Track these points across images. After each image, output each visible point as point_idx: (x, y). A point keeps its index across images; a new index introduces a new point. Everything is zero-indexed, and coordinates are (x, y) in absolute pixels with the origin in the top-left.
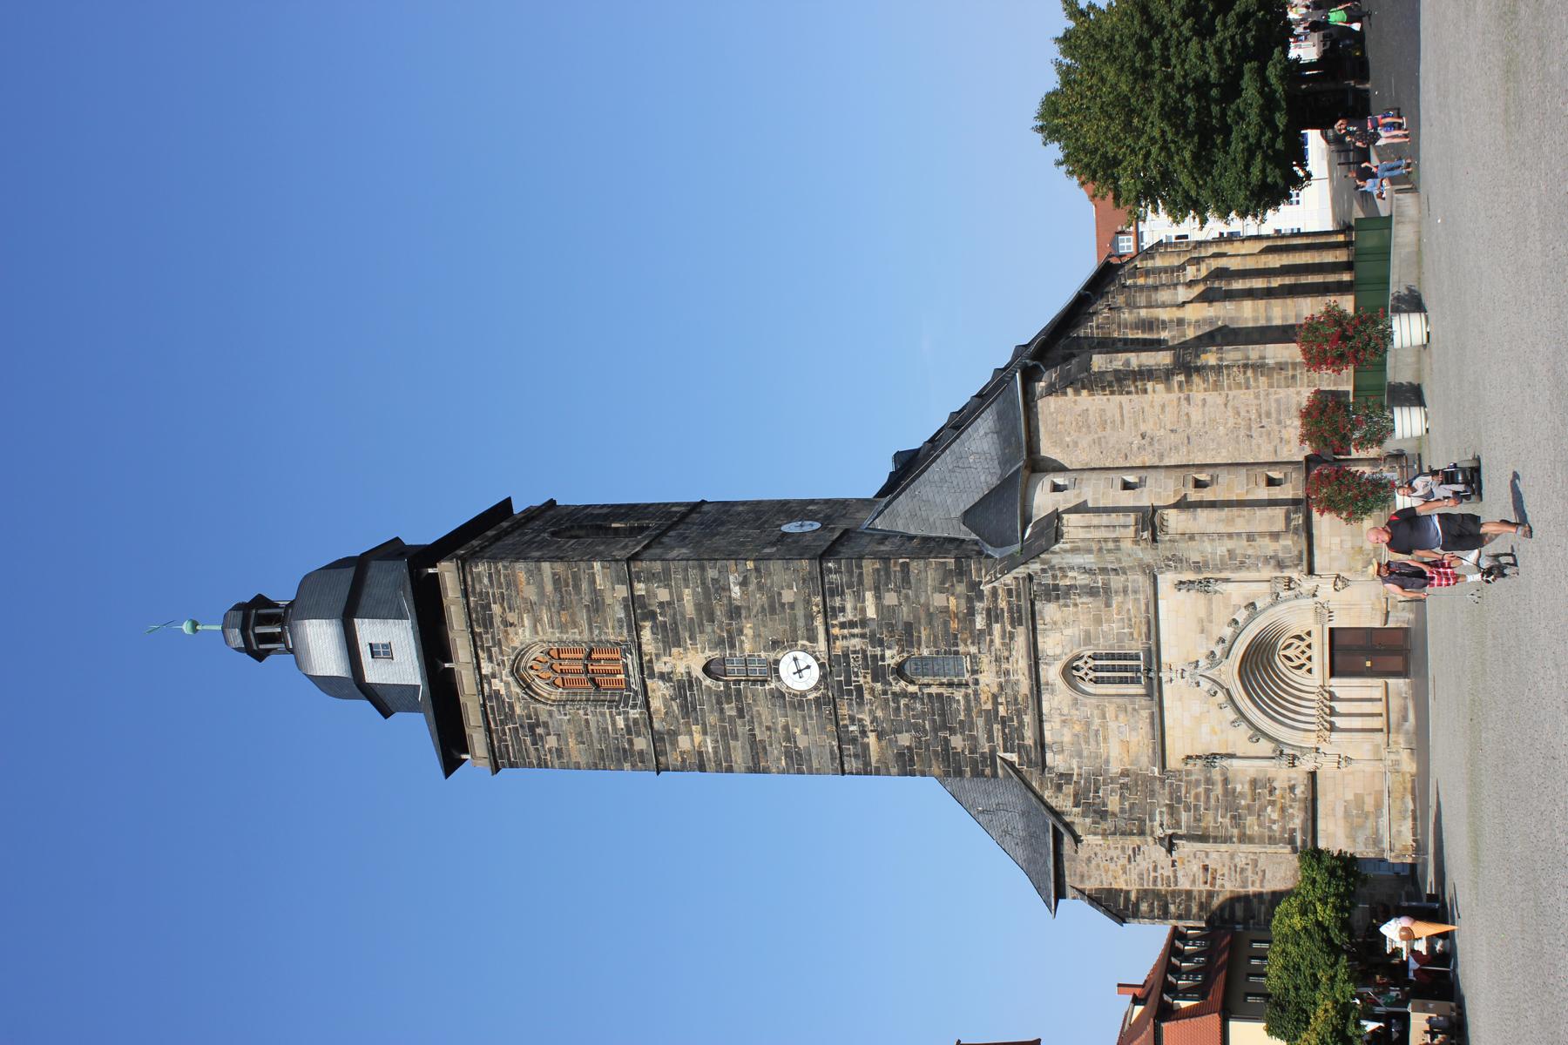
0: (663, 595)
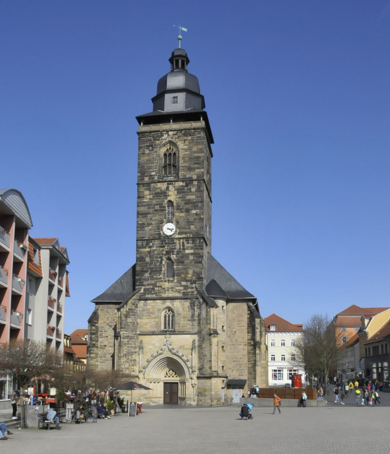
0: (193, 190)
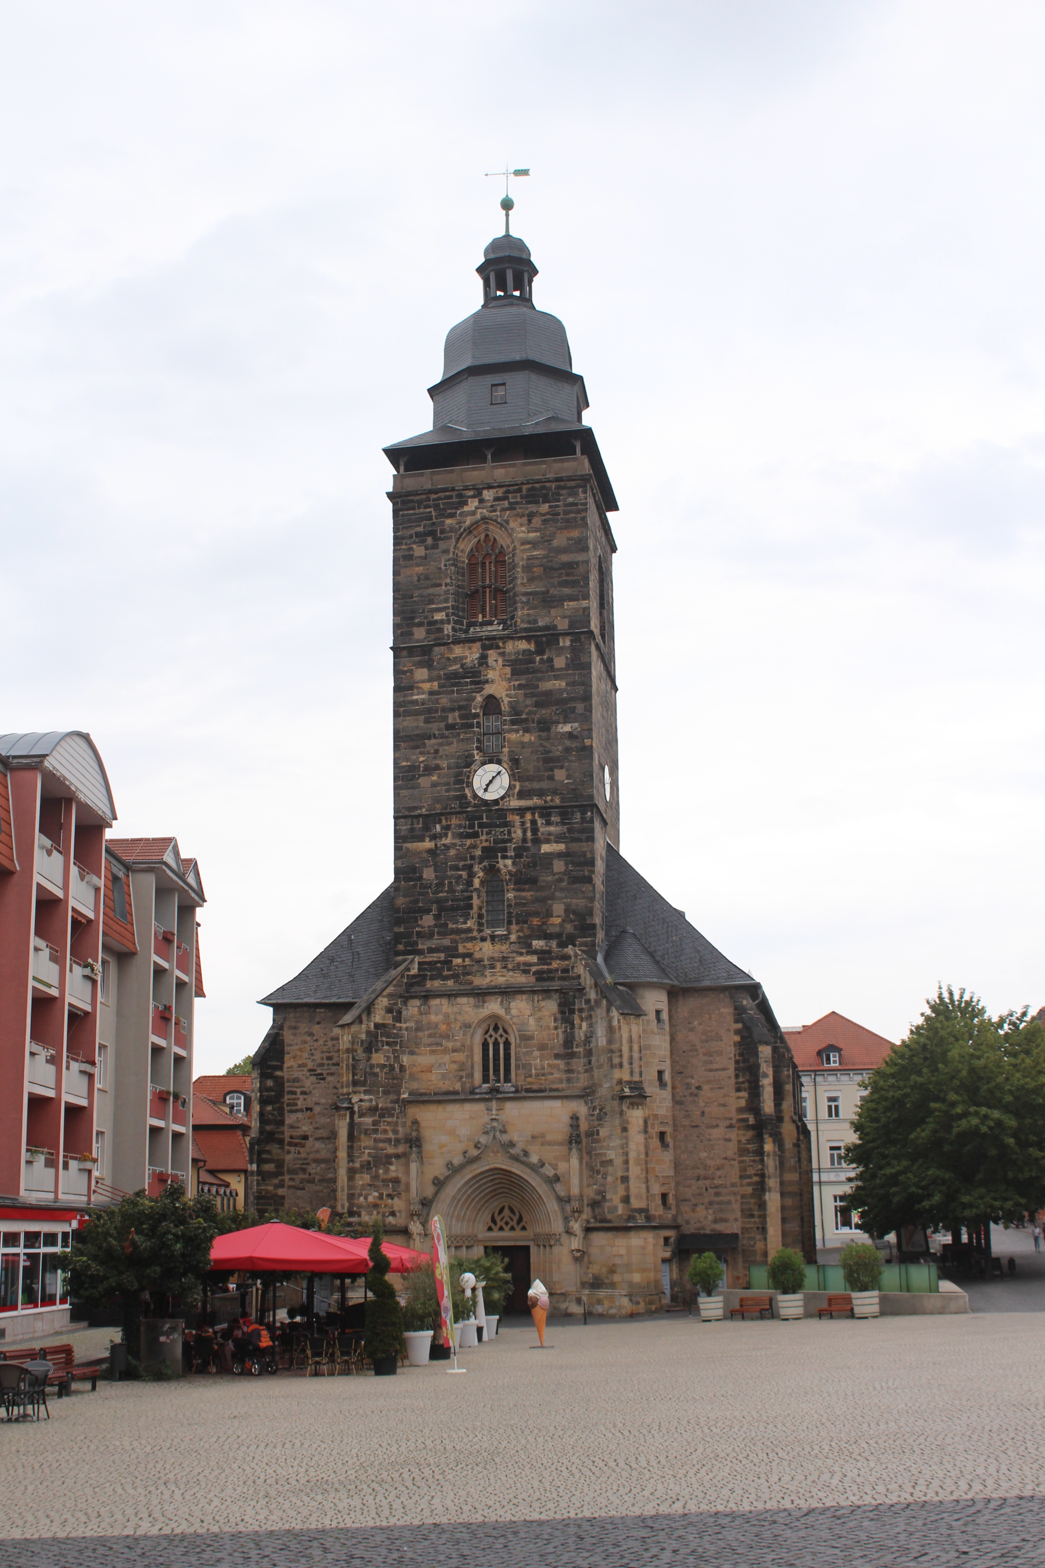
0: (560, 662)
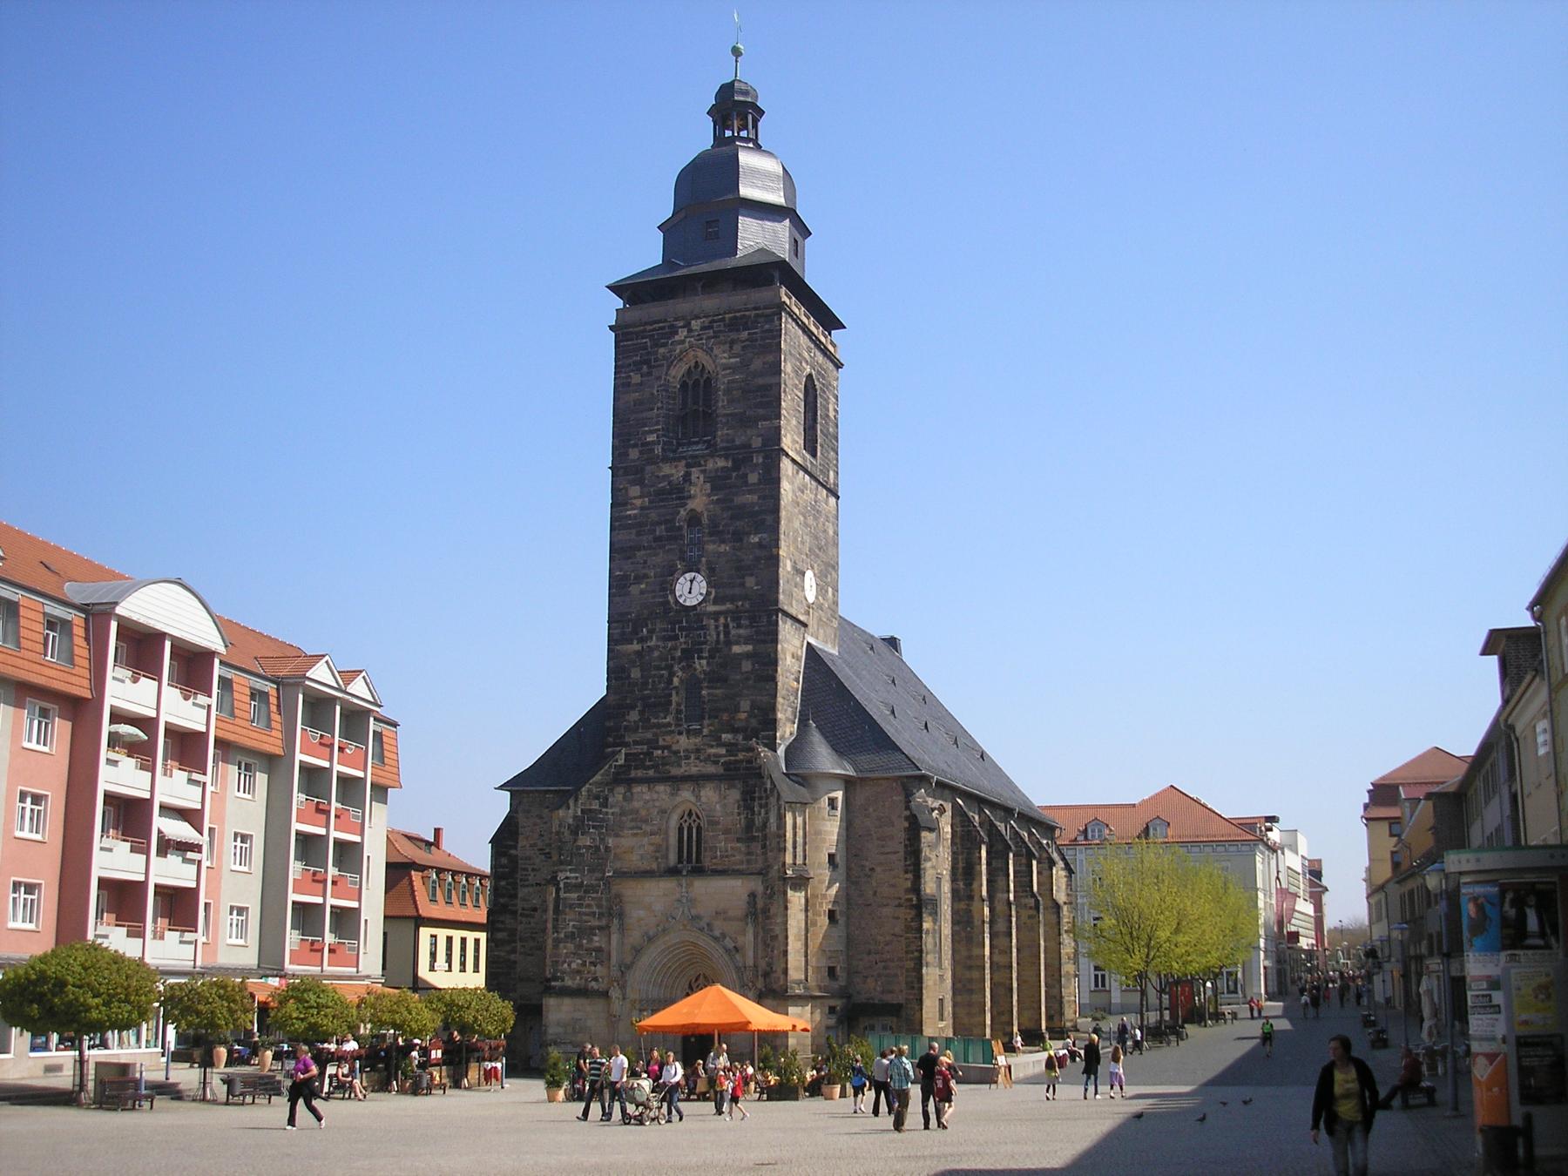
0: (753, 478)
